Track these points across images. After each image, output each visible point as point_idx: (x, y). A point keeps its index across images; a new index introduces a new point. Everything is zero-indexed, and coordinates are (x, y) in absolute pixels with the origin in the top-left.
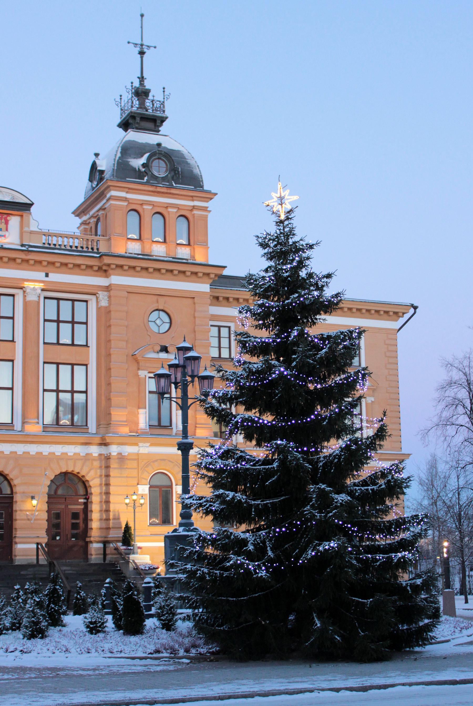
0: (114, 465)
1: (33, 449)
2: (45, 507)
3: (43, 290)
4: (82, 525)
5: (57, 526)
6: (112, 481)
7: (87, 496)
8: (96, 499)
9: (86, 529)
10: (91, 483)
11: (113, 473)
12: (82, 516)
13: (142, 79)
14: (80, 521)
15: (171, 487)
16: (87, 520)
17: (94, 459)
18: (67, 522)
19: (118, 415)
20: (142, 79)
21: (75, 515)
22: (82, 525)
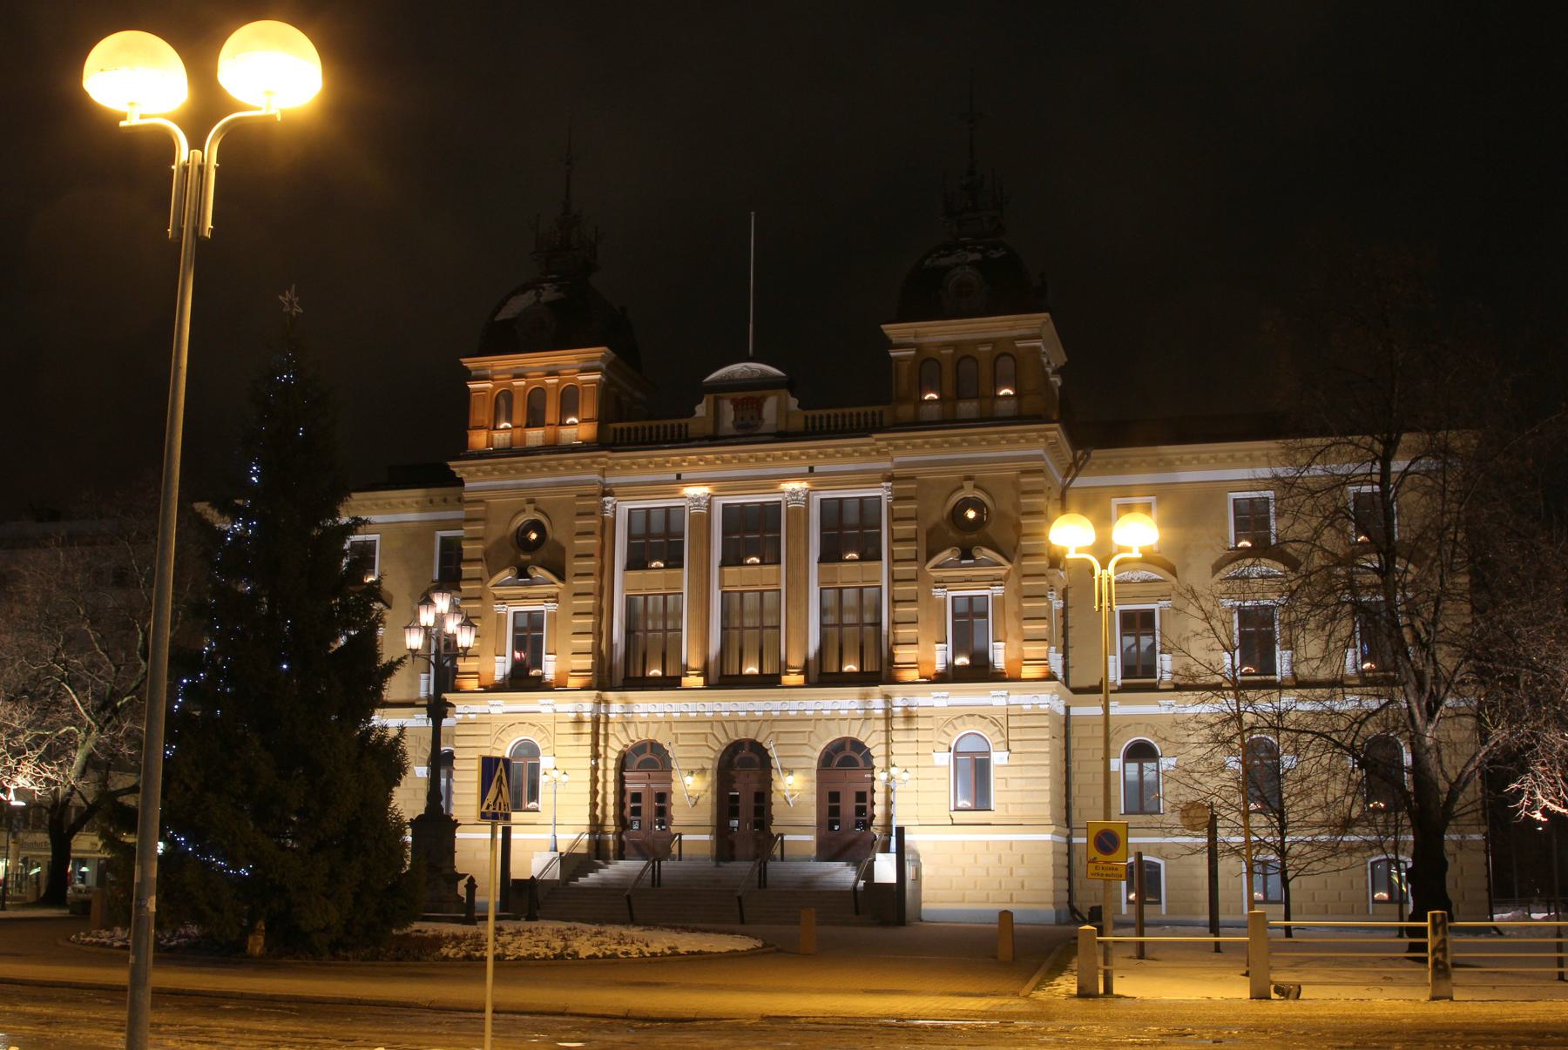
0: (898, 724)
5: (834, 811)
6: (895, 748)
11: (896, 736)
15: (988, 753)
18: (848, 806)
19: (903, 654)
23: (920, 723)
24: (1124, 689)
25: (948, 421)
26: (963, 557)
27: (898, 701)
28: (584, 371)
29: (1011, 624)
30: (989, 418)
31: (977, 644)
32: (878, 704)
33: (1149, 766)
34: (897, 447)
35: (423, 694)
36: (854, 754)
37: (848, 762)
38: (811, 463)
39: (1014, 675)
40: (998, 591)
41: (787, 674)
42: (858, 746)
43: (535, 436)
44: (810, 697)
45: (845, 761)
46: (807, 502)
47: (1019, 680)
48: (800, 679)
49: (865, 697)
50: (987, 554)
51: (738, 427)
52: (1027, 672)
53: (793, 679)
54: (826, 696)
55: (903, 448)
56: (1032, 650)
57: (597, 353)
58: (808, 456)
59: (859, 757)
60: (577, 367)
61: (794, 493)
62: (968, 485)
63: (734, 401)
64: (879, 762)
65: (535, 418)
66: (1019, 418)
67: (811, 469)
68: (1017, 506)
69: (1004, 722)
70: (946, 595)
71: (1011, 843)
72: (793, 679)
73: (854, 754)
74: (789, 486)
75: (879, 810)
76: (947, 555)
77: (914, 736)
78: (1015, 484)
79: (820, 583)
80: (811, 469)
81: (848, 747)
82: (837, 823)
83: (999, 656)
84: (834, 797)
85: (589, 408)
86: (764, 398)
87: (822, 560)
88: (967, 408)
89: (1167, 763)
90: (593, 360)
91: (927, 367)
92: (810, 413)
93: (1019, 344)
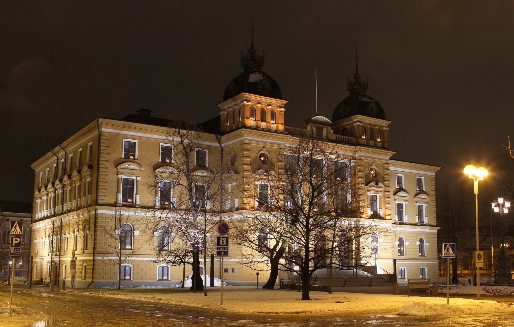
25: (367, 145)
28: (280, 107)
30: (375, 146)
31: (375, 209)
40: (381, 195)
43: (263, 125)
51: (317, 135)
57: (285, 102)
60: (276, 105)
62: (374, 164)
63: (315, 127)
65: (263, 120)
66: (383, 148)
76: (373, 183)
78: (383, 166)
85: (281, 120)
86: (323, 128)
88: (372, 143)
90: (282, 104)
91: (364, 129)
93: (384, 128)
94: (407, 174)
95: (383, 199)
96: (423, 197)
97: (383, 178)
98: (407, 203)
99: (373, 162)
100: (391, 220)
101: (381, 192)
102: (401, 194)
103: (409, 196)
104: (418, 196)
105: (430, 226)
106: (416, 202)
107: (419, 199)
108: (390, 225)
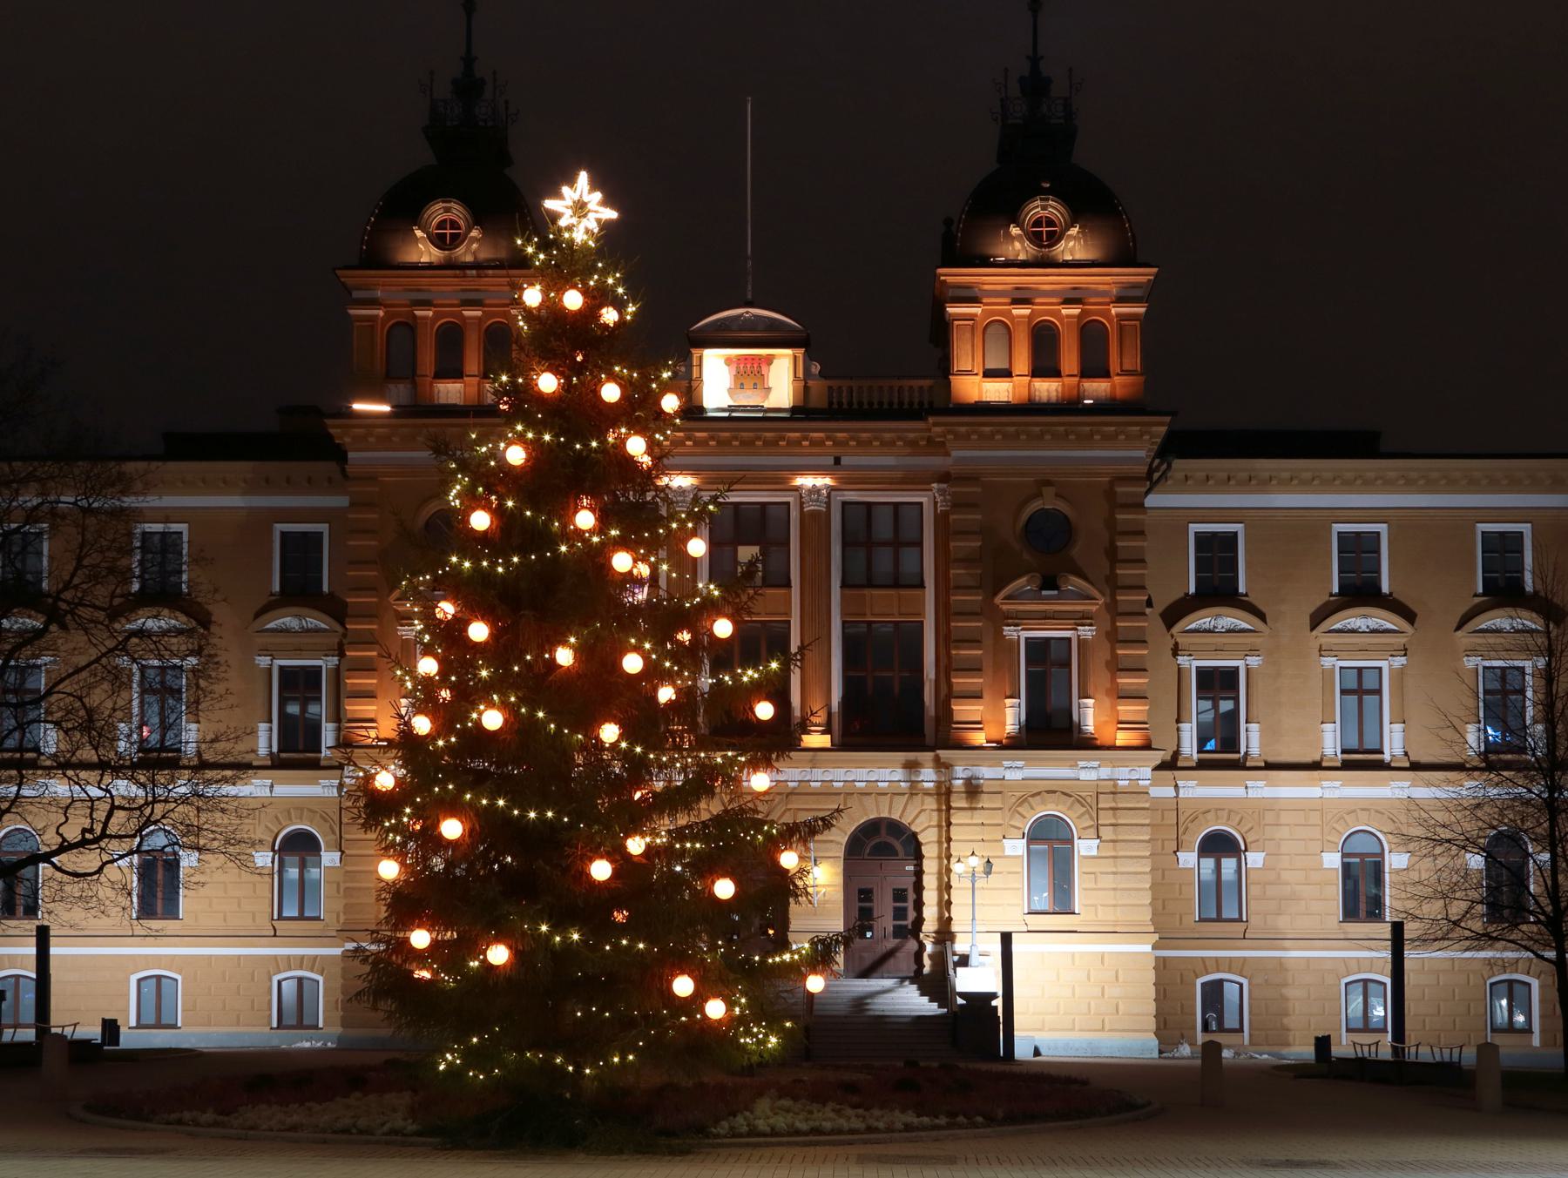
0: (958, 802)
1: (817, 776)
2: (840, 880)
3: (831, 489)
4: (912, 915)
6: (955, 833)
7: (919, 857)
8: (930, 867)
9: (919, 920)
10: (921, 838)
12: (911, 896)
13: (1035, 60)
14: (910, 905)
16: (919, 904)
17: (927, 793)
19: (964, 710)
20: (1035, 60)
21: (900, 895)
22: (912, 915)
23: (985, 801)
24: (1202, 765)
26: (1043, 588)
27: (960, 772)
29: (1099, 678)
32: (928, 776)
33: (1229, 864)
34: (957, 436)
35: (263, 751)
36: (891, 840)
37: (885, 851)
38: (837, 451)
39: (1108, 742)
41: (809, 732)
42: (896, 828)
44: (837, 764)
45: (882, 849)
46: (828, 504)
47: (1114, 748)
48: (823, 741)
49: (911, 766)
50: (1074, 583)
52: (1122, 738)
53: (816, 740)
54: (861, 764)
55: (967, 437)
56: (1128, 710)
58: (837, 443)
59: (897, 845)
61: (815, 490)
62: (1048, 492)
64: (930, 852)
67: (837, 461)
68: (1111, 524)
69: (1103, 804)
70: (1020, 635)
71: (1103, 955)
72: (816, 740)
73: (891, 840)
74: (806, 481)
75: (930, 912)
77: (978, 817)
78: (1110, 494)
79: (843, 614)
80: (837, 461)
81: (883, 831)
82: (870, 929)
83: (1090, 715)
84: (866, 895)
86: (769, 360)
87: (844, 585)
89: (1254, 859)
92: (835, 383)
94: (1400, 520)
95: (1102, 655)
96: (1505, 624)
97: (1113, 555)
98: (1400, 661)
99: (1048, 483)
100: (1147, 747)
101: (1083, 618)
102: (1359, 619)
103: (1402, 624)
104: (1471, 626)
105: (1416, 767)
106: (1471, 652)
107: (1478, 640)
108: (1147, 772)
